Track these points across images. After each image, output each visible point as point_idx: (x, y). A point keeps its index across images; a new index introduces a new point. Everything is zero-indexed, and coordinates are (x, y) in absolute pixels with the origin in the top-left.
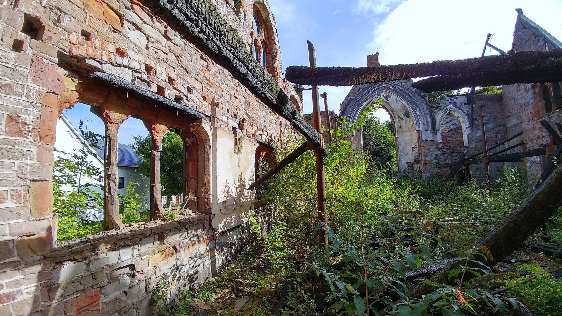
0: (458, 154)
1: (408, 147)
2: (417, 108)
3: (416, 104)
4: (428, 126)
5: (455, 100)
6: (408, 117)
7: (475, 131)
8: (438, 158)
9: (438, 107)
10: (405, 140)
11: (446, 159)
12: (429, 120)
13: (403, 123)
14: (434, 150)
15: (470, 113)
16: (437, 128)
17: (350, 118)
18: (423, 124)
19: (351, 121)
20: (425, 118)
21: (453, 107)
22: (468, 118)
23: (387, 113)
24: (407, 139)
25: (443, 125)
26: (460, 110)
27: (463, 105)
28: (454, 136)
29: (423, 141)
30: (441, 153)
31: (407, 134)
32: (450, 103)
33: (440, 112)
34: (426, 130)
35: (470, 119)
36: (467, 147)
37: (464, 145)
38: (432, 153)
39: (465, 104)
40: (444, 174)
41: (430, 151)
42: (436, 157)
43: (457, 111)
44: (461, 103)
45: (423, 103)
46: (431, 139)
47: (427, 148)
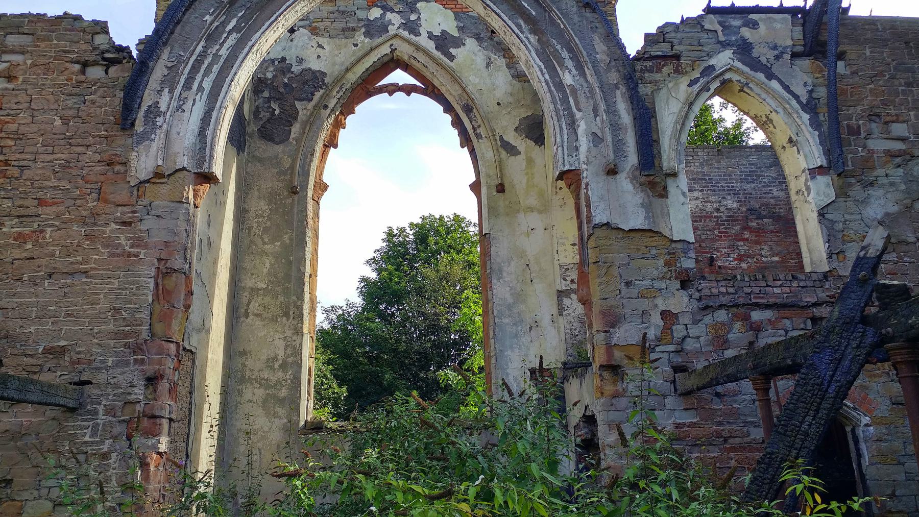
0: (788, 313)
1: (539, 286)
2: (565, 54)
3: (560, 35)
4: (618, 146)
5: (746, 32)
6: (539, 139)
7: (856, 191)
8: (679, 331)
9: (664, 57)
10: (522, 254)
11: (722, 343)
12: (626, 117)
13: (515, 166)
14: (657, 284)
15: (823, 101)
16: (665, 165)
17: (195, 69)
18: (596, 139)
19: (200, 89)
20: (602, 107)
21: (738, 64)
22: (815, 124)
23: (448, 118)
24: (533, 246)
25: (696, 194)
26: (775, 84)
27: (787, 57)
28: (743, 247)
29: (599, 232)
30: (695, 304)
31: (534, 220)
32: (725, 45)
33: (676, 84)
34: (612, 172)
35: (825, 128)
36: (826, 276)
37: (808, 269)
38: (644, 304)
39: (795, 55)
40: (719, 435)
41: (634, 292)
42: (667, 330)
43: (760, 85)
44: (775, 47)
45: (594, 29)
46: (637, 220)
47: (615, 271)
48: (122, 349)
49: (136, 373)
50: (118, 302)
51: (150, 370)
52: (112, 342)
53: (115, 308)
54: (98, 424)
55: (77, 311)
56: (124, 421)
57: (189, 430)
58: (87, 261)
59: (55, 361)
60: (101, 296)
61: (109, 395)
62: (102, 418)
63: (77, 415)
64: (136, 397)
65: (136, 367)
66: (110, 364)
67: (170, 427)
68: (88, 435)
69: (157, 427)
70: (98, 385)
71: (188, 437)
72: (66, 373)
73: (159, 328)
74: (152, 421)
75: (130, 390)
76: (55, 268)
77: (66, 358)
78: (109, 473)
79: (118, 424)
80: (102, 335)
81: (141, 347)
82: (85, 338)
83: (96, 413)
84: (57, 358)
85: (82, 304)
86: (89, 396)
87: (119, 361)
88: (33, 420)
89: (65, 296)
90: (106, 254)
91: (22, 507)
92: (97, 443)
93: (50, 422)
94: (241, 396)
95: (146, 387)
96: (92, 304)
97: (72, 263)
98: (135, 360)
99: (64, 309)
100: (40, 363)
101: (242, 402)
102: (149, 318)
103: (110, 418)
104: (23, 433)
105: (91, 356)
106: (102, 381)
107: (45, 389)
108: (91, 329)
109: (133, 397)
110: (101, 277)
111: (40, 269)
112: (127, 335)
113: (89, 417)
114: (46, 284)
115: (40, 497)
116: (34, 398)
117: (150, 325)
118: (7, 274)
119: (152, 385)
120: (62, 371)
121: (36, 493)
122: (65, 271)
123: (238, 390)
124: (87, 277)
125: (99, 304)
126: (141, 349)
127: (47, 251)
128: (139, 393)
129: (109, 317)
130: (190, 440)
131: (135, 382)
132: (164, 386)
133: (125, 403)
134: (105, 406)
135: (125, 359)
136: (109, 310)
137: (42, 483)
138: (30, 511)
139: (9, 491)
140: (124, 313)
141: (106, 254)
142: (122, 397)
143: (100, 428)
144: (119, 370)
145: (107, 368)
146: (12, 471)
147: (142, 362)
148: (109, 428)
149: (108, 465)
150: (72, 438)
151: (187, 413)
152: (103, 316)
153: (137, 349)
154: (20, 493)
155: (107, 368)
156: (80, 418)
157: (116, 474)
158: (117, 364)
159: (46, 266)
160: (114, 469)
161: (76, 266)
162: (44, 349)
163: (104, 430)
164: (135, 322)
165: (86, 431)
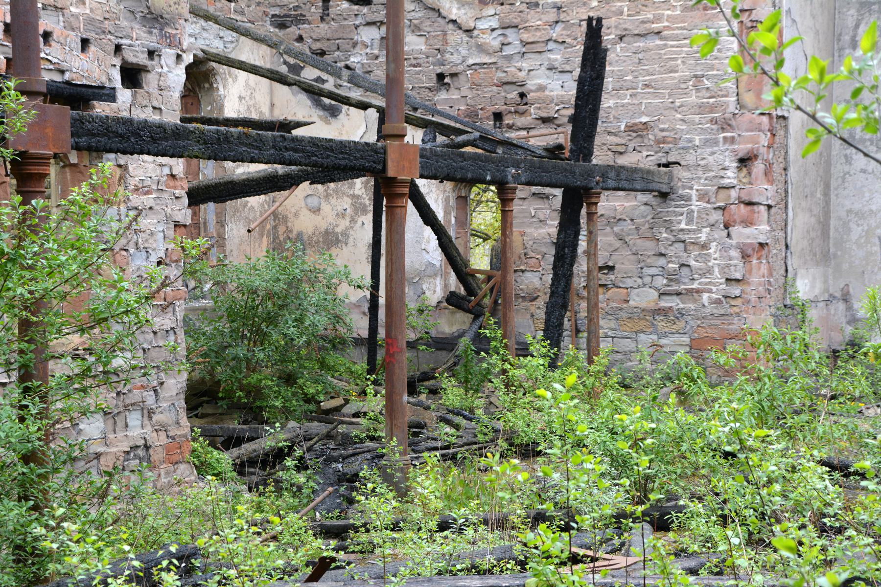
48: (708, 125)
49: (727, 153)
50: (698, 68)
51: (743, 148)
52: (697, 118)
53: (696, 76)
54: (693, 211)
55: (655, 81)
56: (719, 208)
57: (787, 215)
58: (658, 19)
59: (639, 139)
60: (679, 62)
61: (700, 178)
62: (696, 205)
63: (671, 200)
64: (729, 181)
65: (726, 146)
66: (697, 143)
67: (769, 214)
68: (683, 223)
69: (756, 215)
70: (687, 167)
71: (786, 225)
72: (652, 153)
73: (748, 98)
74: (749, 208)
75: (722, 173)
76: (626, 30)
77: (650, 136)
78: (710, 264)
79: (713, 211)
80: (685, 109)
81: (730, 122)
82: (666, 112)
83: (689, 199)
84: (641, 136)
85: (660, 73)
86: (679, 179)
87: (707, 141)
88: (626, 204)
89: (640, 63)
90: (679, 8)
91: (628, 295)
92: (694, 231)
93: (643, 208)
94: (850, 164)
95: (739, 169)
96: (671, 72)
97: (643, 22)
98: (725, 138)
99: (641, 78)
100: (624, 142)
101: (852, 173)
102: (735, 87)
103: (705, 205)
104: (618, 218)
105: (676, 134)
106: (691, 163)
107: (645, 176)
108: (672, 102)
109: (726, 181)
110: (676, 38)
111: (609, 31)
112: (712, 109)
113: (683, 202)
114: (619, 50)
115: (644, 285)
116: (638, 187)
117: (738, 95)
118: (575, 39)
119: (746, 166)
120: (648, 151)
121: (639, 281)
122: (636, 32)
123: (846, 156)
124: (661, 39)
125: (676, 72)
126: (729, 125)
127: (614, 9)
128: (731, 176)
129: (691, 88)
130: (789, 228)
131: (727, 164)
132: (758, 167)
133: (719, 188)
134: (697, 190)
135: (714, 137)
136: (689, 78)
137: (644, 270)
138: (637, 299)
139: (613, 277)
140: (706, 82)
141: (679, 8)
142: (715, 181)
143: (695, 214)
144: (709, 150)
145: (695, 148)
146: (613, 257)
147: (732, 140)
148: (704, 216)
149: (709, 255)
150: (668, 226)
151: (783, 195)
152: (683, 86)
153: (725, 125)
154: (624, 280)
155: (695, 148)
156: (673, 203)
157: (719, 265)
158: (706, 143)
159: (616, 27)
160: (715, 259)
161: (647, 26)
162: (626, 126)
163: (699, 217)
164: (720, 93)
165: (681, 218)
